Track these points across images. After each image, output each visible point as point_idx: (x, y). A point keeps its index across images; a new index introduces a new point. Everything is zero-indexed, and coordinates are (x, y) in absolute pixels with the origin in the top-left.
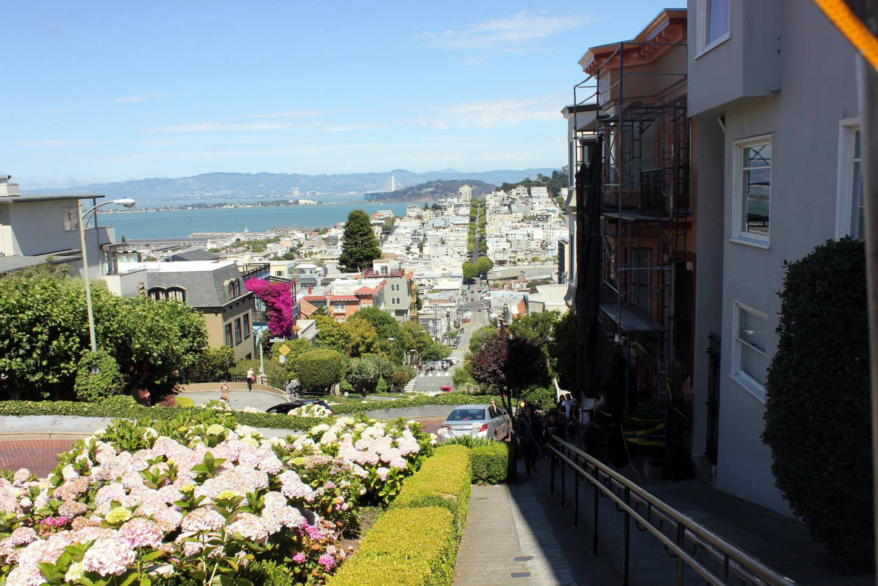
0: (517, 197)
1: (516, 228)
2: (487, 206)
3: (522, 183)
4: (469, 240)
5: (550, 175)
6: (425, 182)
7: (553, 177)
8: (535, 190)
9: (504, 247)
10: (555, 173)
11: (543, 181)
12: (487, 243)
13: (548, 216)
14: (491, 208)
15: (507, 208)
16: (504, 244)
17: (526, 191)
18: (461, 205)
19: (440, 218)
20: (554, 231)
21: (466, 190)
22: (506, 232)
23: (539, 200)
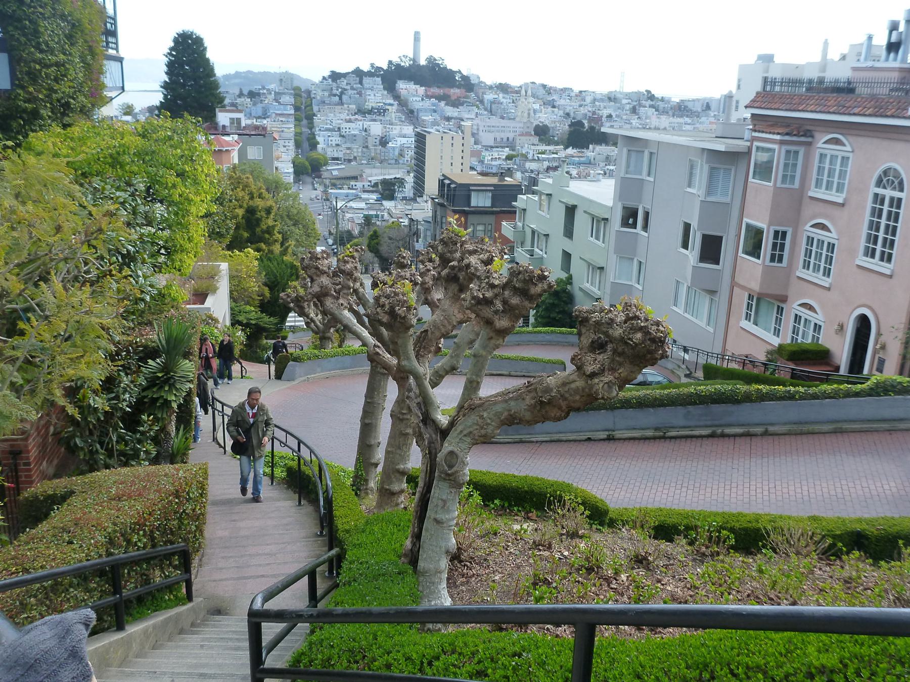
0: (348, 87)
1: (350, 121)
2: (313, 96)
3: (353, 72)
4: (296, 133)
5: (385, 67)
6: (233, 72)
7: (389, 67)
8: (366, 80)
9: (337, 143)
10: (390, 62)
11: (375, 72)
12: (317, 137)
13: (385, 111)
14: (318, 98)
15: (337, 98)
16: (336, 139)
17: (358, 81)
18: (284, 94)
19: (260, 105)
20: (394, 127)
22: (338, 126)
23: (375, 92)
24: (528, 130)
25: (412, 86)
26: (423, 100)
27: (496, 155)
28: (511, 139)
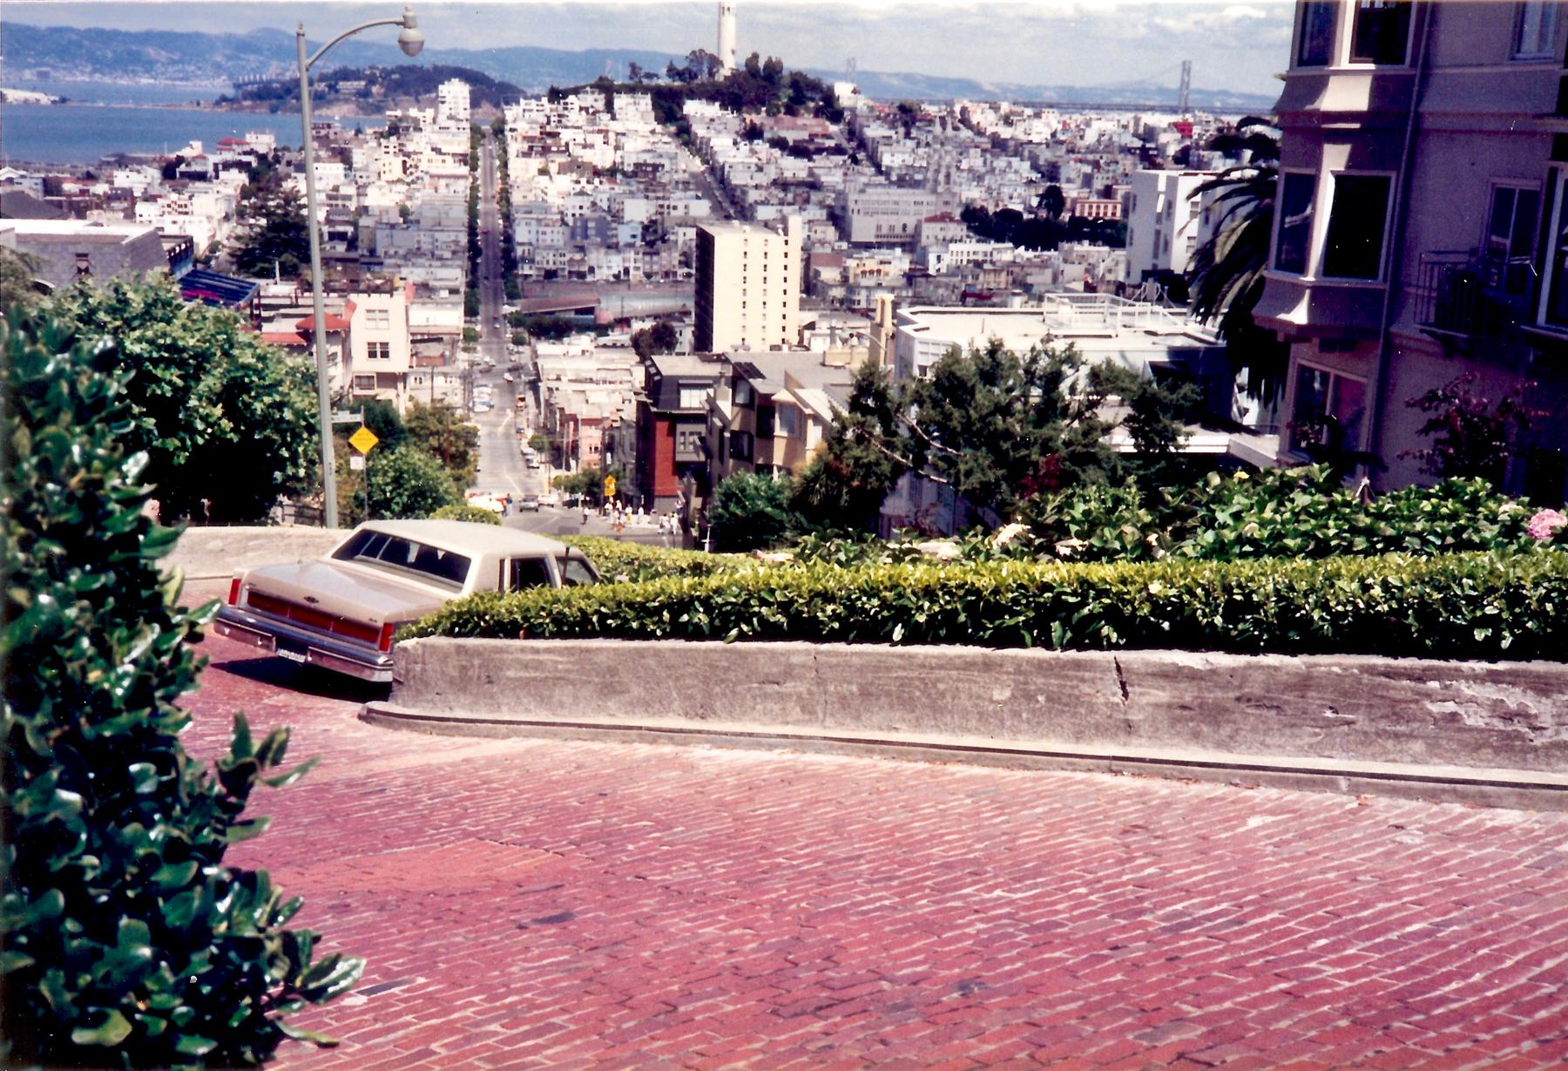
3: (592, 86)
8: (620, 101)
17: (600, 105)
21: (456, 93)
24: (947, 209)
25: (714, 110)
26: (735, 143)
27: (871, 265)
28: (910, 230)
